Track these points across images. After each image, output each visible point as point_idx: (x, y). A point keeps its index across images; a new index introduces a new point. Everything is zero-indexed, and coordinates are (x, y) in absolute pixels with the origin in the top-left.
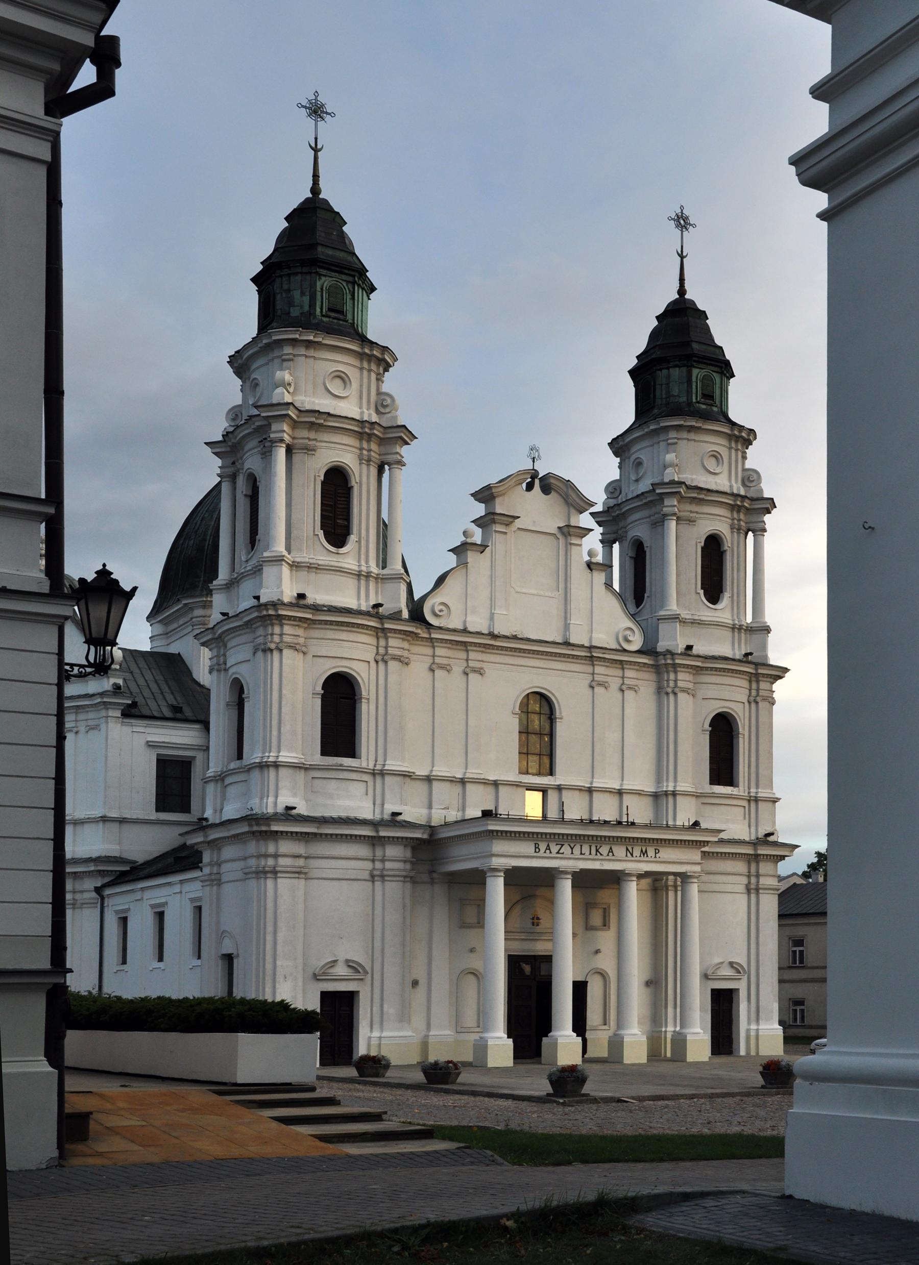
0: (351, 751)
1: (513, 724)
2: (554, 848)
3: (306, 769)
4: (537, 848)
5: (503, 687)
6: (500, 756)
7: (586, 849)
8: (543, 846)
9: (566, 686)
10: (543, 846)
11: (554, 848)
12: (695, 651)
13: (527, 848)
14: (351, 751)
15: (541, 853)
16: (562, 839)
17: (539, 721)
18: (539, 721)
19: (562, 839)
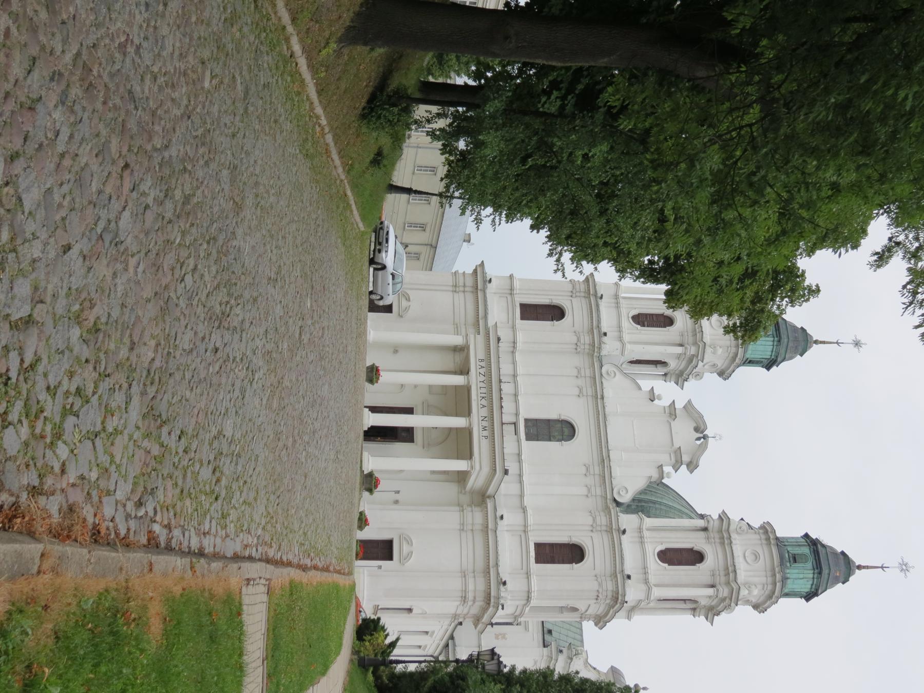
0: (523, 317)
1: (553, 416)
2: (482, 371)
3: (513, 352)
4: (482, 360)
5: (573, 409)
6: (535, 406)
7: (484, 390)
8: (483, 364)
9: (579, 449)
10: (483, 364)
11: (482, 371)
12: (624, 537)
13: (481, 355)
14: (523, 317)
15: (478, 363)
16: (488, 375)
17: (556, 430)
18: (556, 430)
19: (488, 375)
